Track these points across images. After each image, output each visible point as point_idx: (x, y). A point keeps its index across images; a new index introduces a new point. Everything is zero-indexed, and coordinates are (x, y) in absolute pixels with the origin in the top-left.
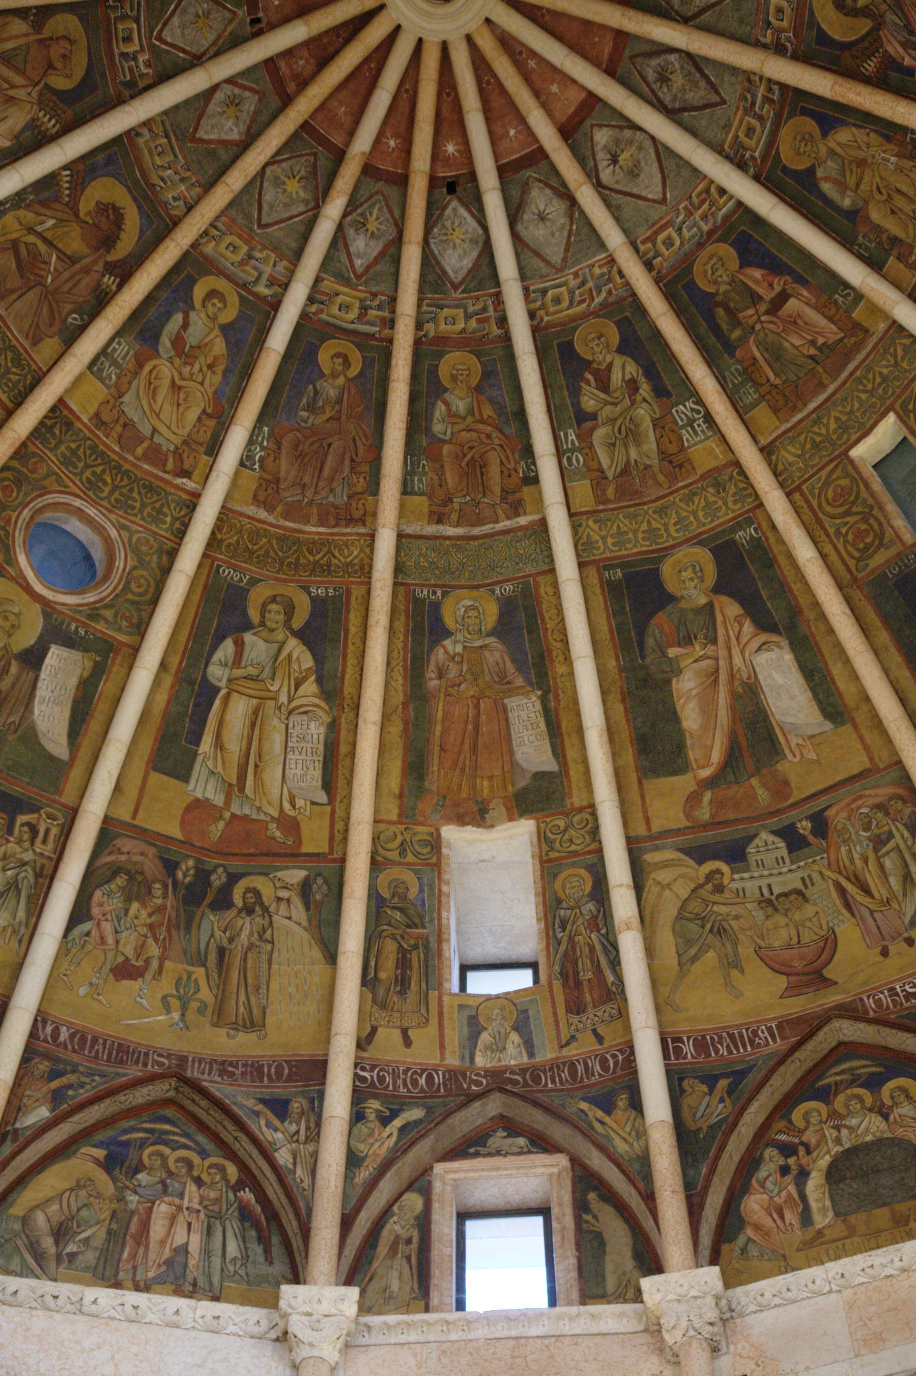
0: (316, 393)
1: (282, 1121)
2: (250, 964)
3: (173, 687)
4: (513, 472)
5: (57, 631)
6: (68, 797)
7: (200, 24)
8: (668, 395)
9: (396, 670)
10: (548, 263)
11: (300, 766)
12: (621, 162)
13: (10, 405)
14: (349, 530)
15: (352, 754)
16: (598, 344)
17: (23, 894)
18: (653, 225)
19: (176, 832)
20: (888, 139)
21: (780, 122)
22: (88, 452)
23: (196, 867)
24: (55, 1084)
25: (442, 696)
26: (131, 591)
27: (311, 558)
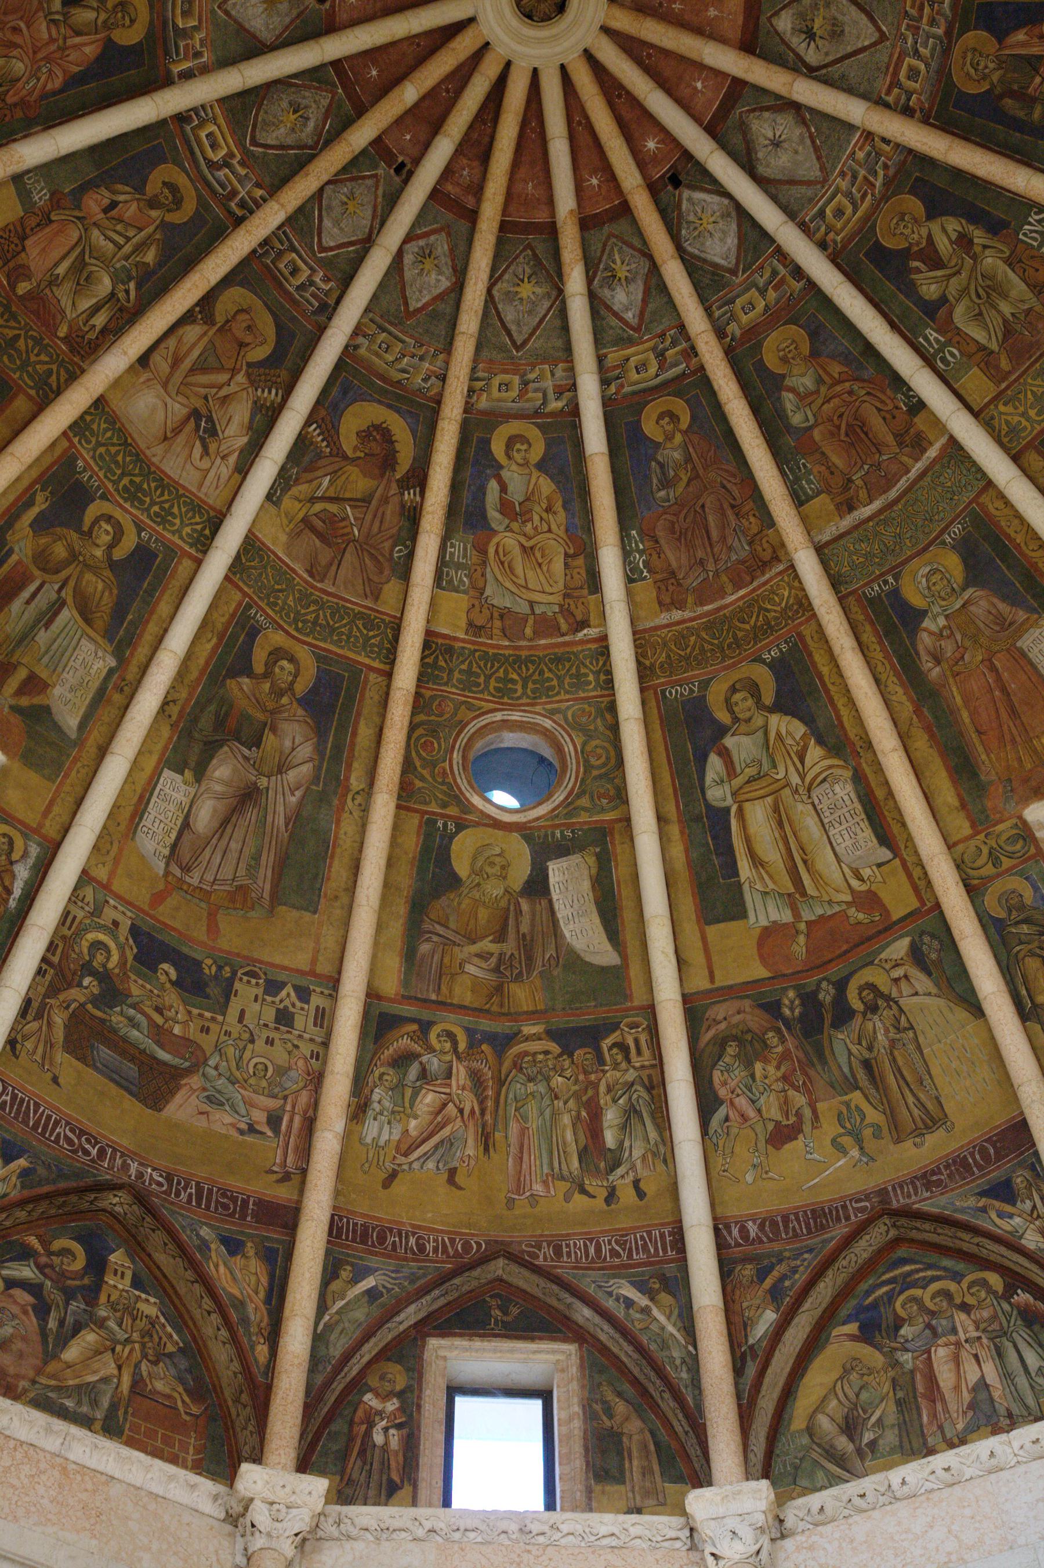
0: (661, 466)
1: (1014, 1204)
2: (900, 1061)
3: (682, 833)
4: (895, 412)
5: (545, 846)
6: (639, 999)
7: (351, 209)
9: (889, 683)
10: (808, 183)
11: (846, 837)
13: (387, 668)
14: (767, 576)
15: (890, 794)
16: (906, 225)
17: (645, 1115)
18: (888, 68)
19: (763, 973)
22: (482, 664)
23: (799, 996)
24: (768, 1282)
25: (951, 680)
26: (592, 767)
27: (747, 627)
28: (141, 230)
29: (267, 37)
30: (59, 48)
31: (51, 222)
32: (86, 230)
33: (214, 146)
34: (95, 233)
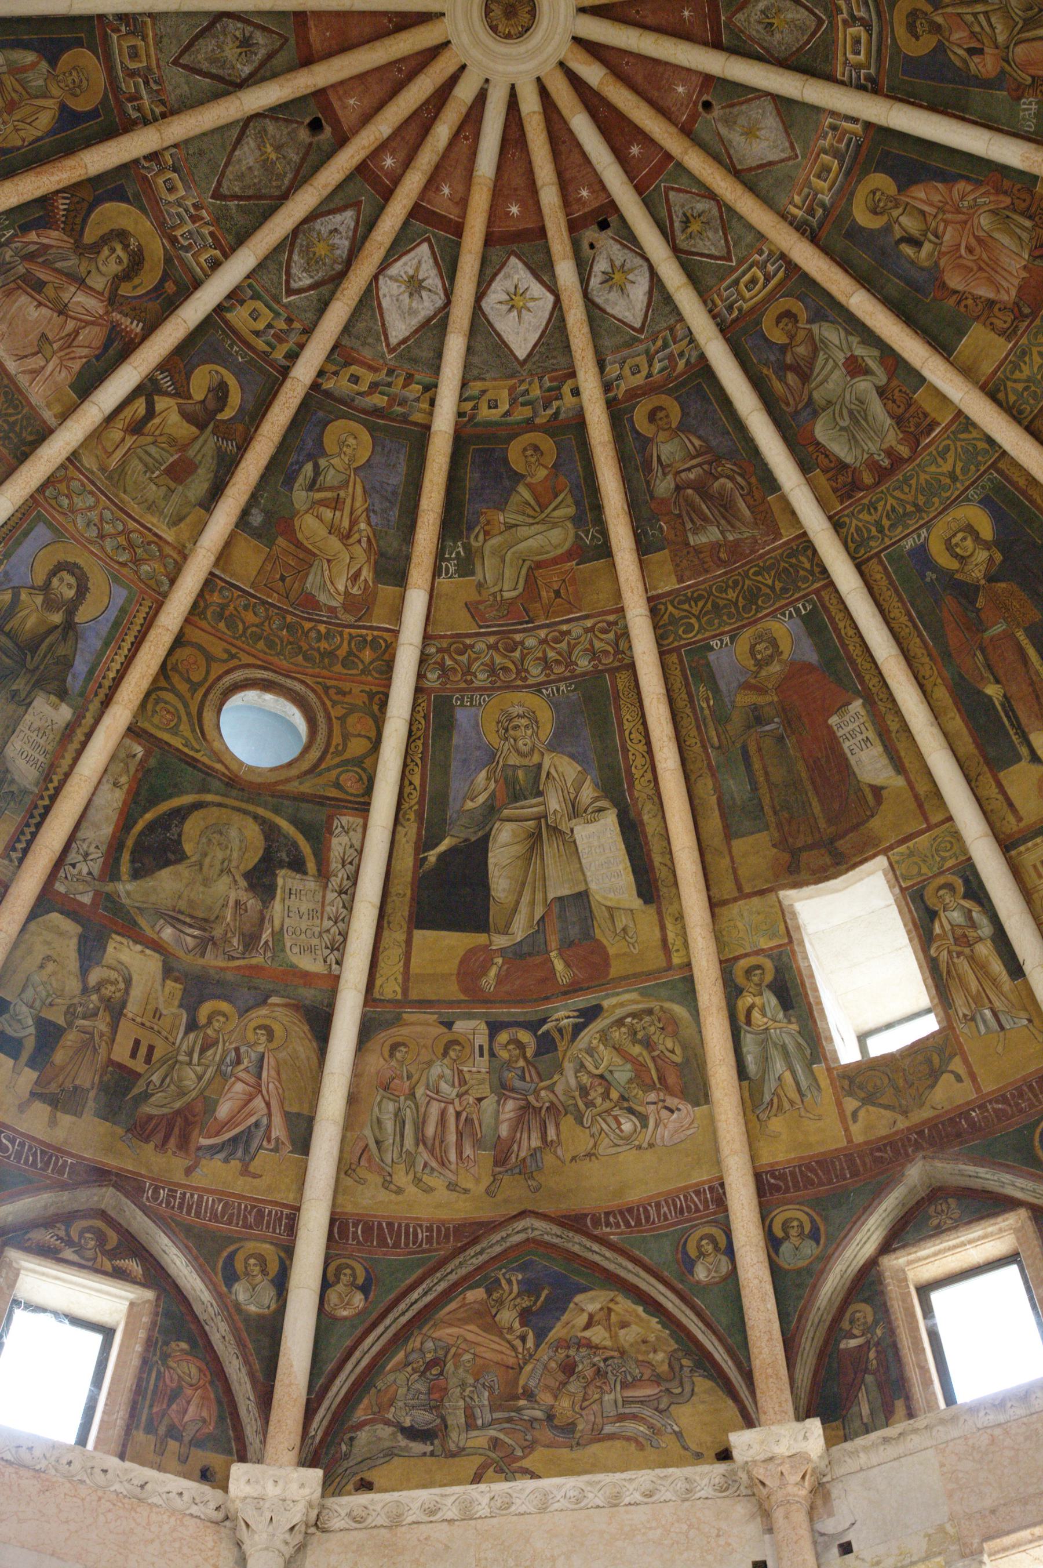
21: (111, 83)
28: (959, 14)
29: (770, 107)
30: (944, 212)
31: (1033, 77)
32: (1008, 47)
33: (857, 41)
34: (1001, 39)
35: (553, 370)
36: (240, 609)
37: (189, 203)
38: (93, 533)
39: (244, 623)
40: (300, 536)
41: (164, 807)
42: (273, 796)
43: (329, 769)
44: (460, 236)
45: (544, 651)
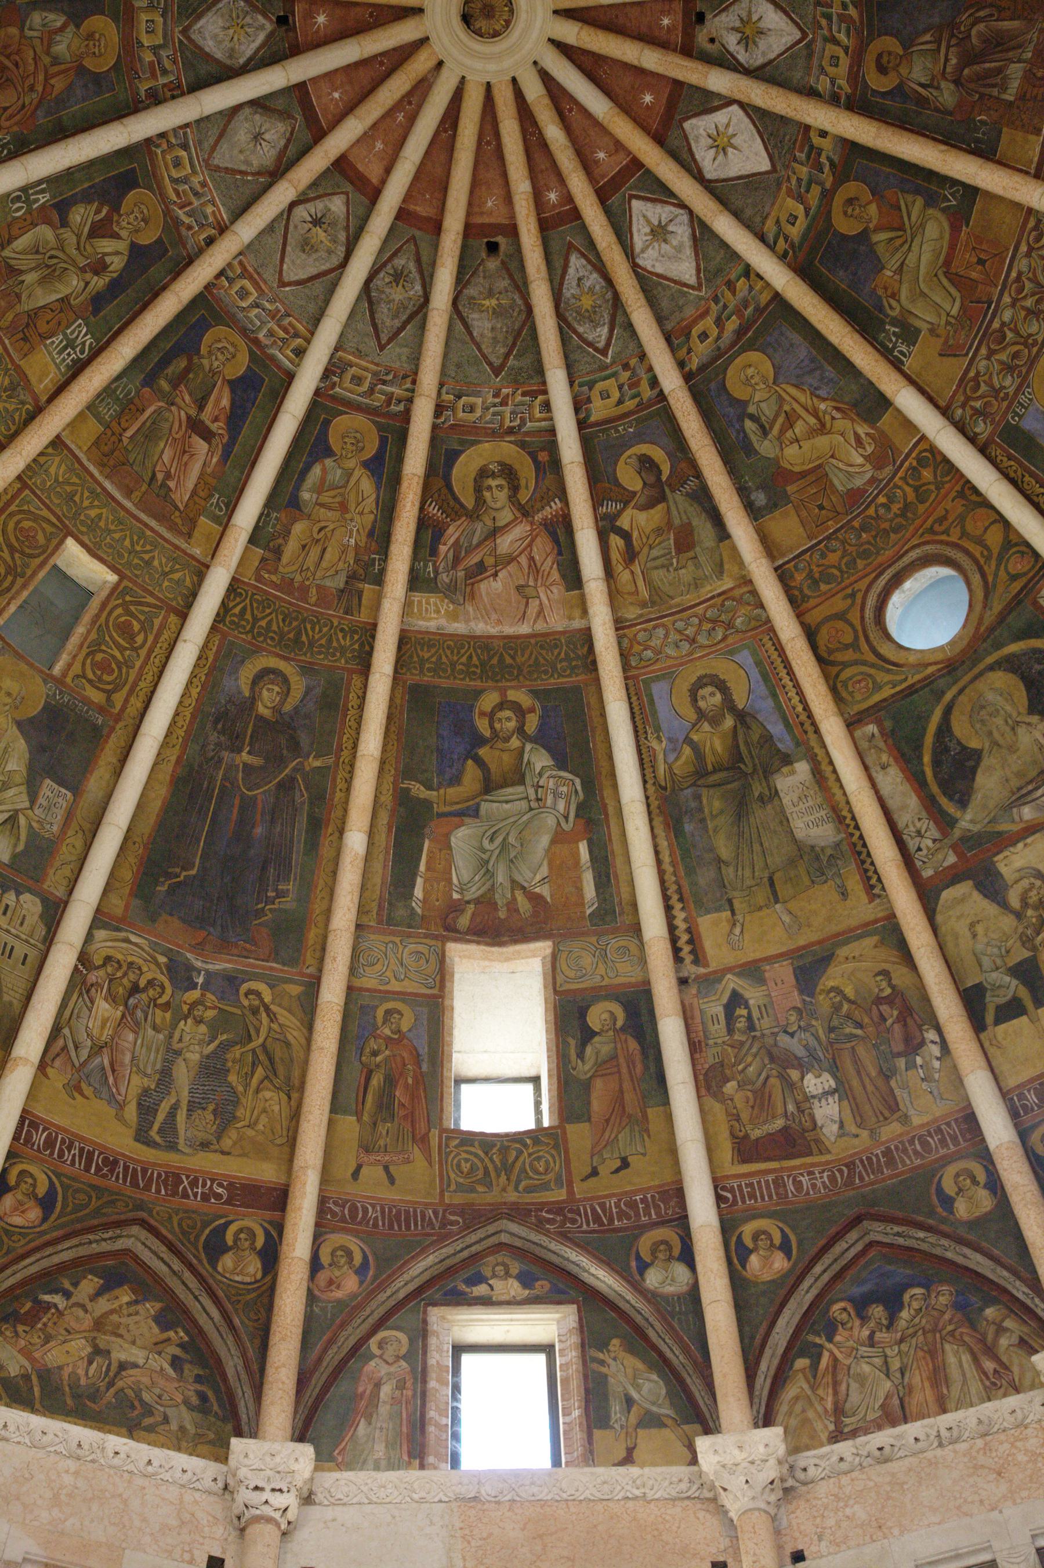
8: (96, 312)
12: (314, 230)
18: (258, 274)
20: (371, 534)
21: (369, 414)
35: (794, 143)
36: (821, 562)
37: (490, 400)
38: (685, 646)
39: (834, 567)
40: (797, 469)
41: (929, 740)
42: (985, 641)
43: (996, 575)
44: (643, 166)
45: (1023, 308)
